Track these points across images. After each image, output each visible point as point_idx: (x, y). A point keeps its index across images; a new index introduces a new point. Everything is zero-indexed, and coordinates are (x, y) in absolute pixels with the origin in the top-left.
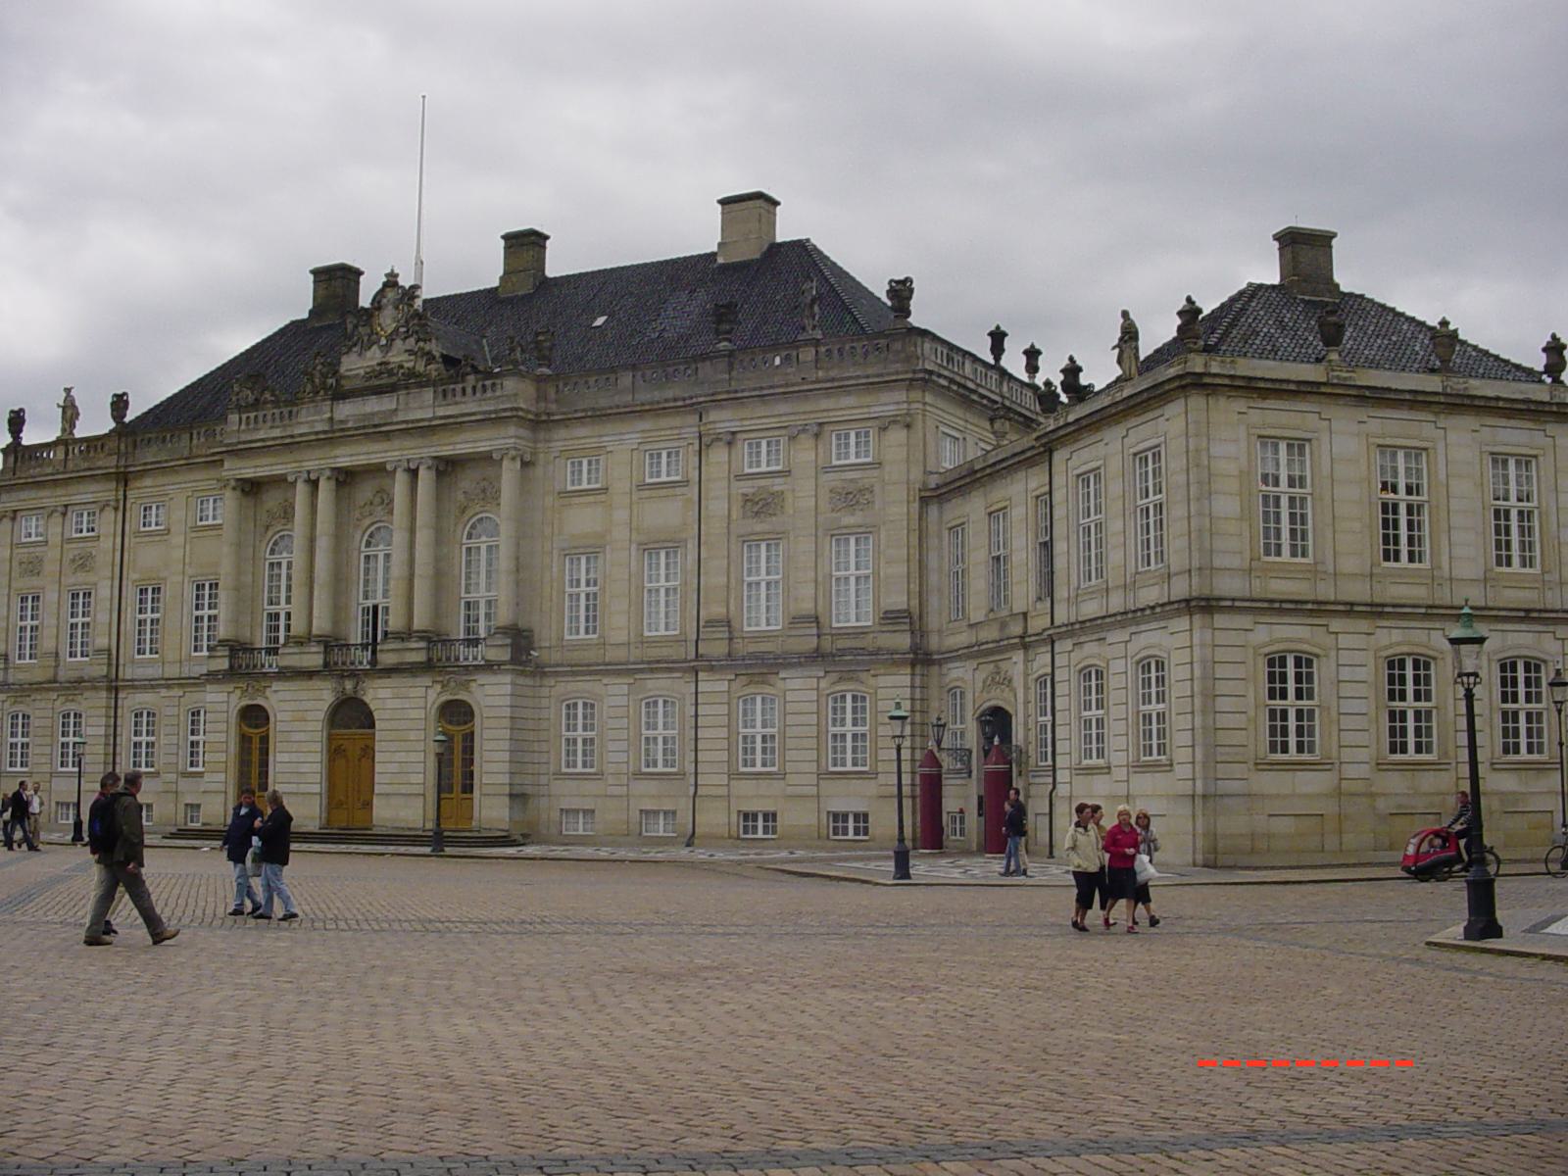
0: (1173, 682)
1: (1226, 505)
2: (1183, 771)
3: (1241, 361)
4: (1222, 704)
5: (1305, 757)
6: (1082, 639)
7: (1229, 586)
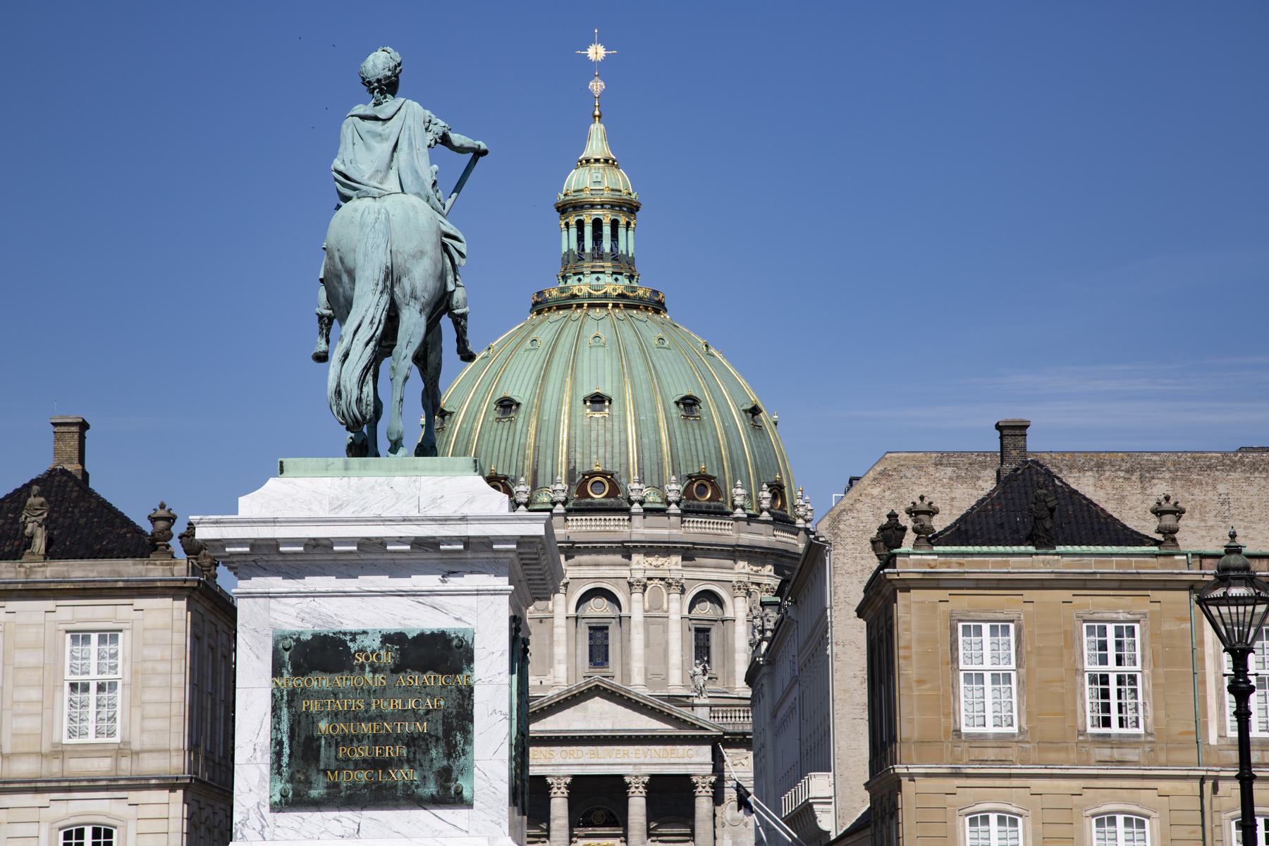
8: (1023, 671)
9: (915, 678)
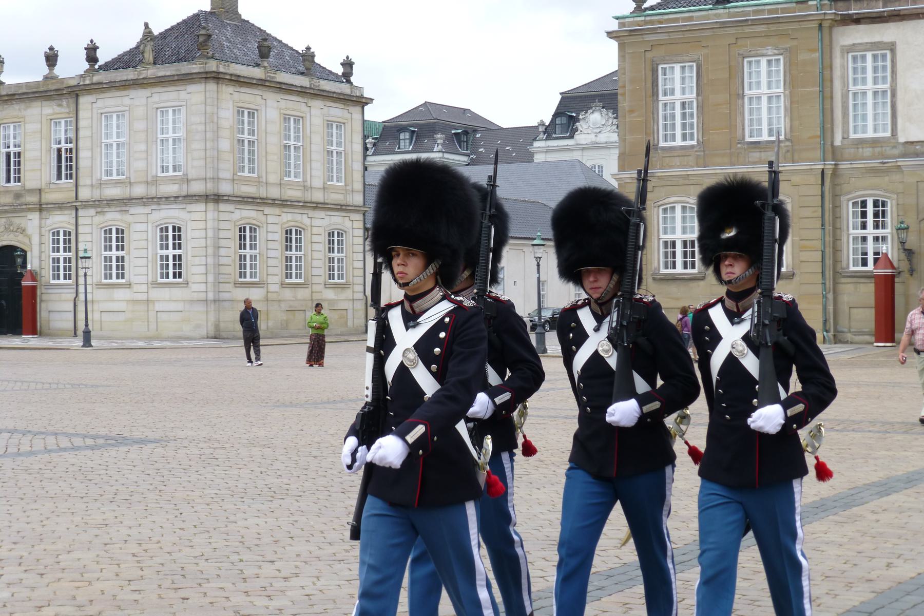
0: (189, 238)
1: (225, 145)
2: (194, 287)
3: (232, 65)
4: (223, 252)
5: (120, 281)
6: (106, 210)
7: (225, 188)
8: (700, 98)
9: (627, 109)
